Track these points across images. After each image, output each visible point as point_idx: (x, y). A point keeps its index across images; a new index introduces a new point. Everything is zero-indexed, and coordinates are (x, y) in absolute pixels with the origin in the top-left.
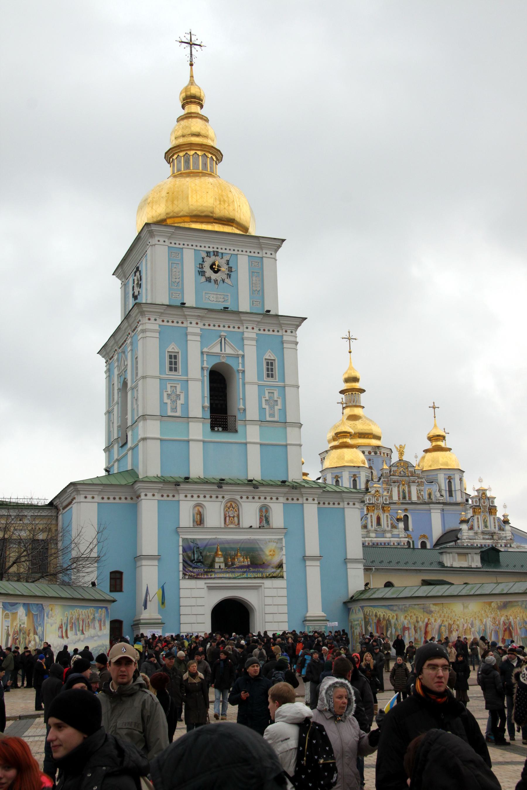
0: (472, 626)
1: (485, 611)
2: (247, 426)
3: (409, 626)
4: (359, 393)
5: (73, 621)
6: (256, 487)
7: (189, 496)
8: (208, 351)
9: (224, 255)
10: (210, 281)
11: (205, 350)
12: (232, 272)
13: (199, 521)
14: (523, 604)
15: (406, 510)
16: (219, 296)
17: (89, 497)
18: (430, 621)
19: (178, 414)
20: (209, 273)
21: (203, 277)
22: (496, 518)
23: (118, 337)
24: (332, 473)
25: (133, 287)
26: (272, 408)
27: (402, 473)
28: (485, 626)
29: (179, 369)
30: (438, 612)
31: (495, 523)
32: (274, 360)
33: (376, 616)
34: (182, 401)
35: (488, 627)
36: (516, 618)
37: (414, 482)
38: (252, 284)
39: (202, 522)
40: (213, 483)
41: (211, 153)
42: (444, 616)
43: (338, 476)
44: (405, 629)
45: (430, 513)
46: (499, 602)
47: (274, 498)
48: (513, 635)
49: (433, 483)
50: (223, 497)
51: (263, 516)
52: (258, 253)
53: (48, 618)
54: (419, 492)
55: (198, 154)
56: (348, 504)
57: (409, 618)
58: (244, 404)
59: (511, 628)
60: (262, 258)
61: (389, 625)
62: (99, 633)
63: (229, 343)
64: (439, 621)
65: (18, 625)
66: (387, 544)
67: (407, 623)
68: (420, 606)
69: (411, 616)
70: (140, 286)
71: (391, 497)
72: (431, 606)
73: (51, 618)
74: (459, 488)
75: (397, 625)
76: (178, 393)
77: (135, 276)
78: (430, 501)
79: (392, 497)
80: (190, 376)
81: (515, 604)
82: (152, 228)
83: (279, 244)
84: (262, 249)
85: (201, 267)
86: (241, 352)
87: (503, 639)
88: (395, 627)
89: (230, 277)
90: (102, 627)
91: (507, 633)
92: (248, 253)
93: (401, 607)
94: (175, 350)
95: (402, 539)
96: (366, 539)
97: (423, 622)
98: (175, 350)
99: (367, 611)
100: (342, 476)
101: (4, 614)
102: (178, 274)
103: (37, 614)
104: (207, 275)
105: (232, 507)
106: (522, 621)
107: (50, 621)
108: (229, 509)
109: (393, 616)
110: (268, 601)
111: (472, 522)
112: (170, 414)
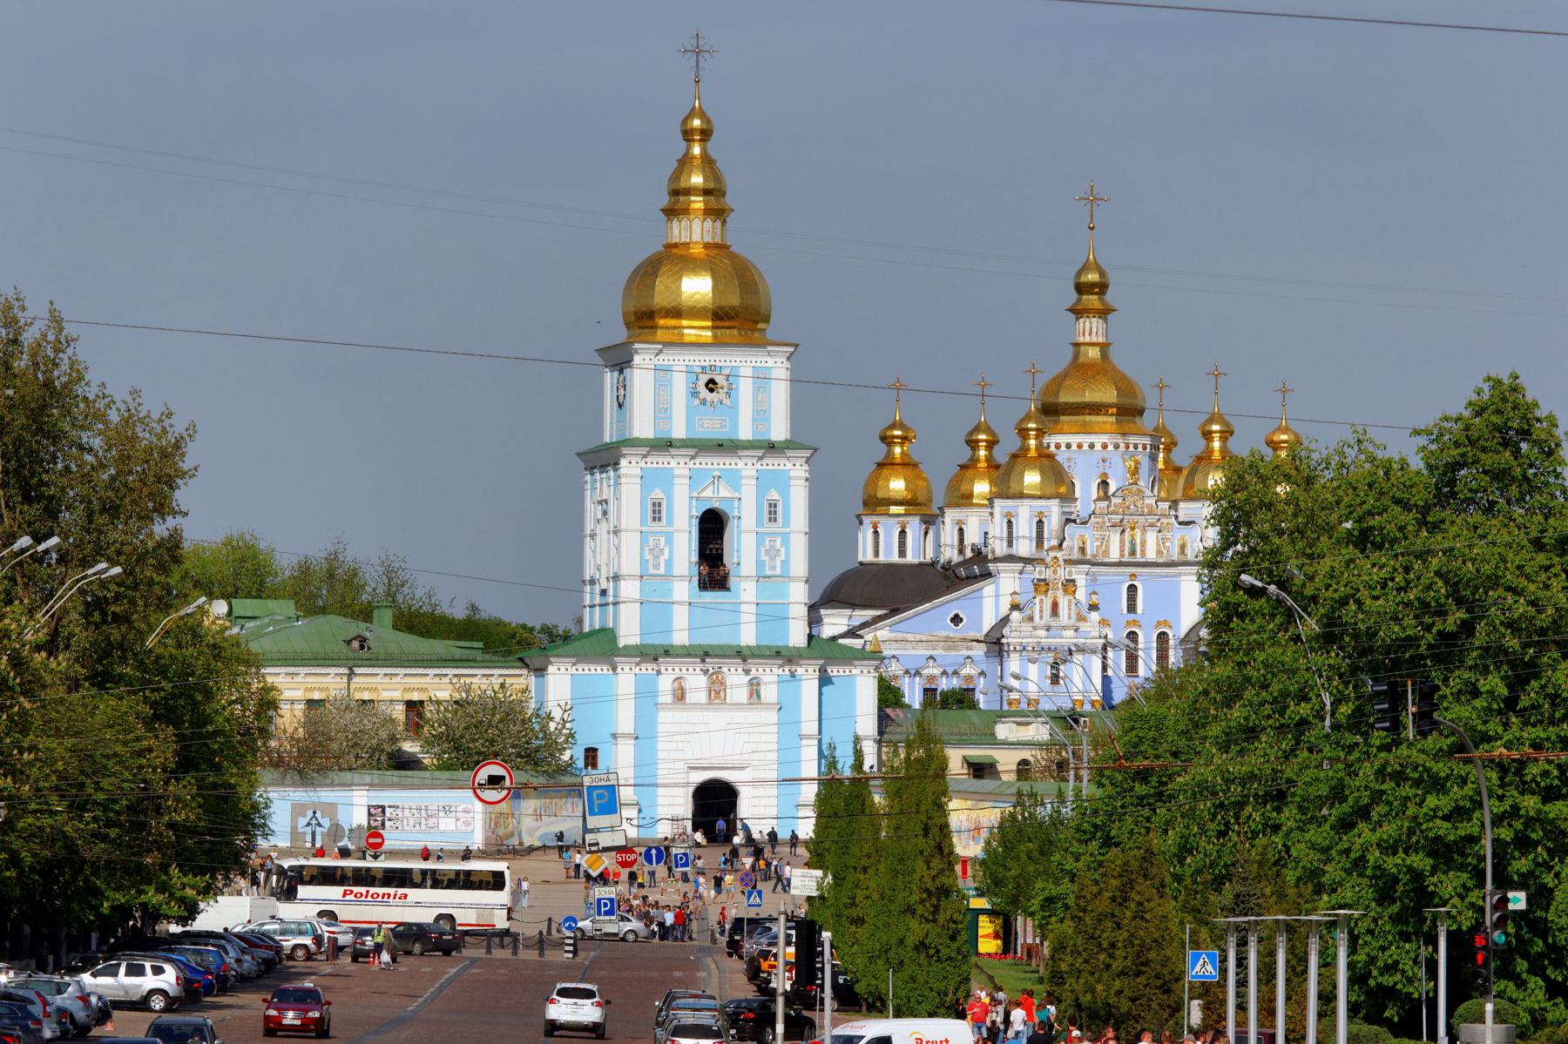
6: (745, 660)
11: (695, 494)
15: (1133, 576)
17: (563, 668)
20: (704, 393)
26: (773, 558)
37: (1152, 525)
40: (695, 656)
47: (768, 670)
58: (738, 557)
70: (625, 387)
71: (1106, 553)
78: (1183, 558)
86: (737, 495)
92: (754, 364)
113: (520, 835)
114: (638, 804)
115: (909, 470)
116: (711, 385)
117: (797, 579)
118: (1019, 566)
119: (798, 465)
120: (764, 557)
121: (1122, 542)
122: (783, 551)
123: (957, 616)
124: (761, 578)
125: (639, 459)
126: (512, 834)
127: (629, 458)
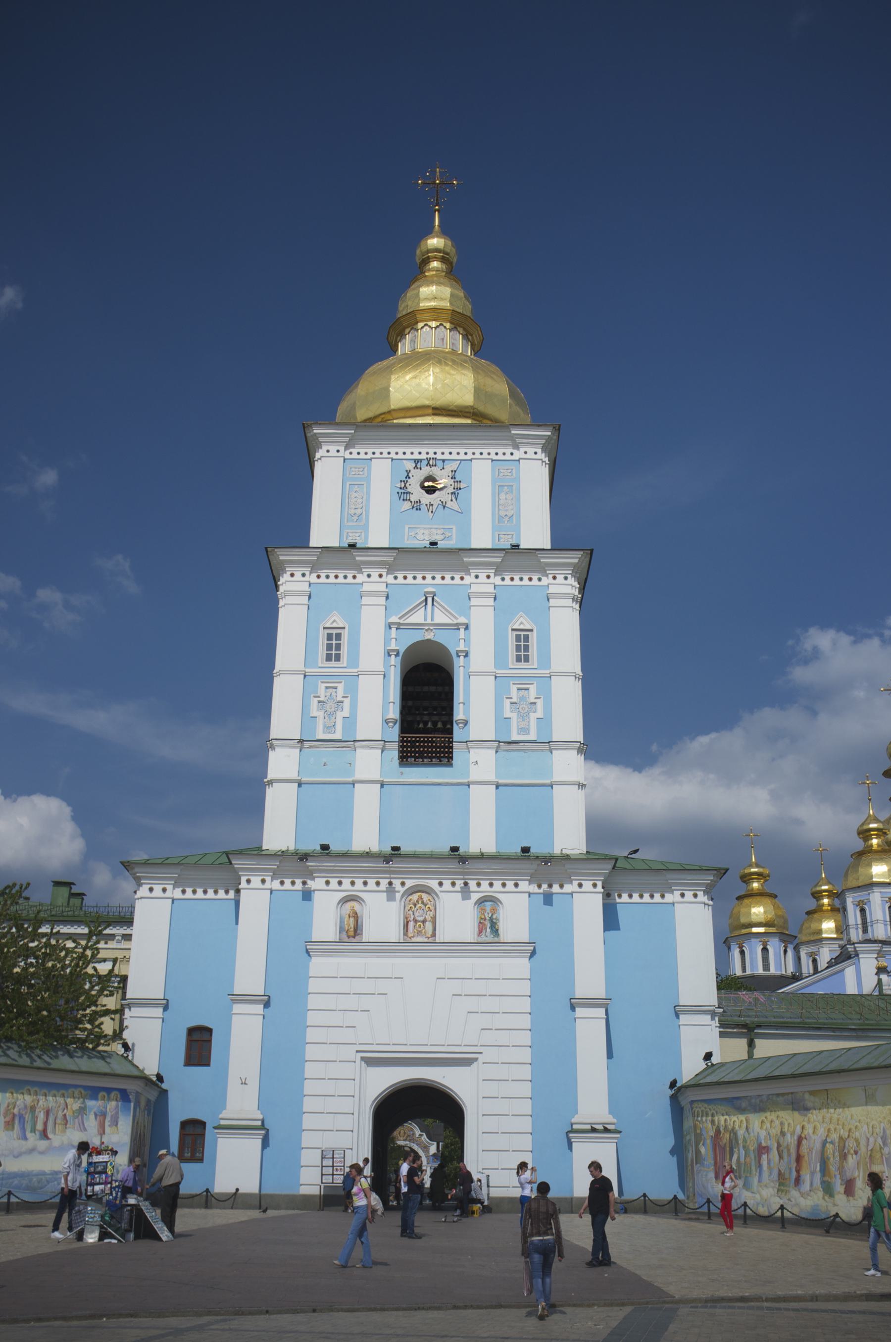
0: (885, 1143)
2: (471, 751)
5: (16, 1111)
7: (334, 882)
8: (398, 621)
9: (446, 462)
11: (394, 619)
12: (460, 489)
13: (352, 929)
16: (434, 531)
18: (805, 1132)
19: (338, 736)
20: (417, 493)
21: (406, 502)
24: (853, 897)
26: (524, 716)
29: (343, 658)
32: (531, 630)
34: (346, 713)
38: (496, 504)
39: (358, 932)
42: (831, 1119)
43: (863, 901)
44: (762, 1150)
47: (510, 885)
50: (403, 884)
51: (485, 919)
52: (512, 454)
56: (683, 895)
58: (467, 711)
61: (733, 1141)
63: (441, 605)
64: (823, 1129)
67: (766, 1137)
68: (786, 1096)
69: (772, 1121)
72: (807, 1096)
75: (748, 1142)
76: (339, 698)
80: (364, 665)
82: (315, 431)
83: (549, 433)
84: (516, 447)
85: (403, 485)
86: (462, 620)
88: (744, 1147)
90: (107, 1129)
93: (753, 1101)
94: (338, 624)
98: (338, 624)
100: (870, 901)
102: (360, 501)
104: (413, 498)
105: (423, 903)
108: (415, 905)
109: (742, 1121)
110: (492, 1089)
112: (321, 736)
114: (263, 1127)
115: (767, 900)
117: (564, 745)
118: (876, 947)
119: (560, 578)
120: (507, 714)
122: (540, 703)
124: (504, 744)
125: (307, 571)
127: (289, 570)
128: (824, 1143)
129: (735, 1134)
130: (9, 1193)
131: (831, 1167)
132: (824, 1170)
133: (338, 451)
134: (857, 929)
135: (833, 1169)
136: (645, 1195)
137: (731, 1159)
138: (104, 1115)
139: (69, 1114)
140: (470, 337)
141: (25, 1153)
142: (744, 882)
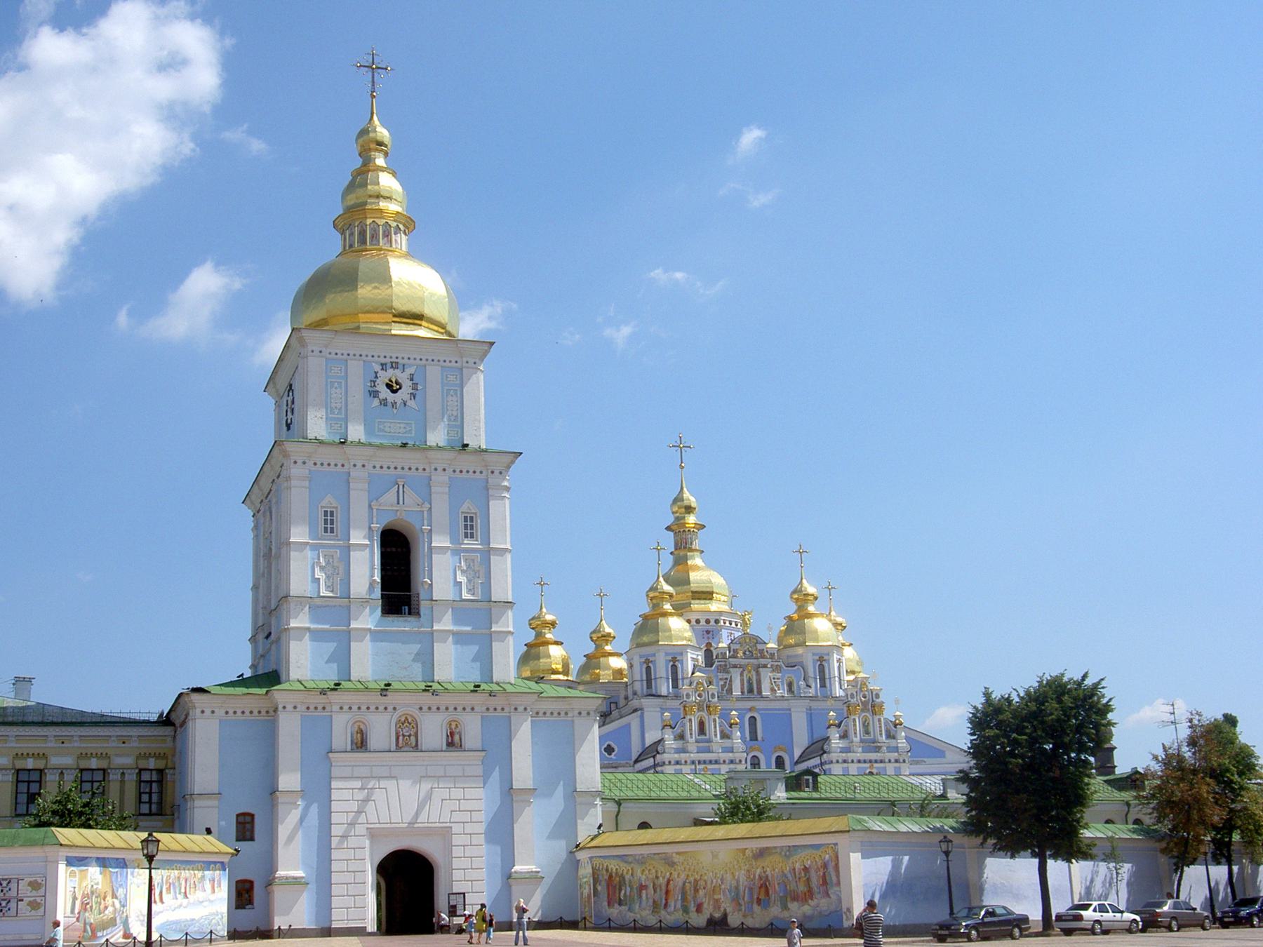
1: (738, 861)
3: (647, 883)
4: (695, 530)
5: (171, 881)
10: (385, 405)
13: (360, 742)
14: (782, 850)
15: (750, 710)
17: (208, 712)
18: (672, 877)
20: (385, 393)
21: (376, 399)
22: (882, 719)
23: (263, 481)
24: (641, 657)
25: (287, 411)
27: (747, 653)
28: (738, 881)
30: (683, 863)
31: (880, 727)
33: (607, 870)
35: (741, 883)
36: (774, 870)
37: (765, 666)
39: (364, 743)
41: (394, 221)
42: (689, 870)
44: (642, 887)
45: (790, 714)
46: (754, 849)
48: (770, 893)
49: (796, 667)
50: (395, 709)
52: (456, 362)
53: (133, 877)
54: (773, 681)
55: (377, 224)
57: (647, 872)
59: (767, 884)
60: (461, 369)
61: (622, 883)
62: (212, 897)
64: (683, 875)
65: (90, 886)
66: (713, 762)
68: (660, 855)
69: (649, 870)
71: (730, 691)
72: (674, 855)
73: (138, 877)
74: (837, 674)
76: (335, 564)
77: (288, 396)
79: (731, 689)
81: (774, 851)
83: (486, 348)
85: (373, 385)
87: (758, 898)
88: (629, 886)
89: (414, 398)
90: (216, 891)
91: (763, 890)
95: (737, 755)
96: (683, 755)
97: (664, 878)
99: (596, 866)
100: (655, 661)
101: (69, 872)
103: (117, 872)
104: (382, 396)
105: (408, 722)
106: (781, 873)
107: (135, 880)
111: (846, 726)
113: (126, 923)
116: (393, 387)
120: (458, 580)
121: (742, 681)
123: (609, 745)
126: (112, 922)
128: (684, 884)
129: (624, 878)
130: (187, 934)
131: (688, 897)
132: (684, 899)
133: (321, 352)
134: (642, 685)
135: (689, 898)
136: (561, 918)
137: (620, 893)
138: (214, 881)
139: (196, 880)
140: (407, 231)
141: (177, 908)
142: (533, 628)
